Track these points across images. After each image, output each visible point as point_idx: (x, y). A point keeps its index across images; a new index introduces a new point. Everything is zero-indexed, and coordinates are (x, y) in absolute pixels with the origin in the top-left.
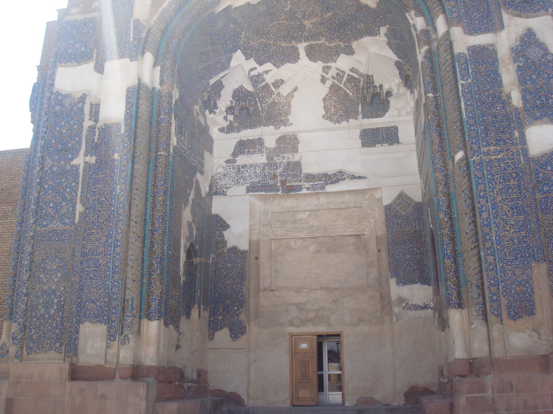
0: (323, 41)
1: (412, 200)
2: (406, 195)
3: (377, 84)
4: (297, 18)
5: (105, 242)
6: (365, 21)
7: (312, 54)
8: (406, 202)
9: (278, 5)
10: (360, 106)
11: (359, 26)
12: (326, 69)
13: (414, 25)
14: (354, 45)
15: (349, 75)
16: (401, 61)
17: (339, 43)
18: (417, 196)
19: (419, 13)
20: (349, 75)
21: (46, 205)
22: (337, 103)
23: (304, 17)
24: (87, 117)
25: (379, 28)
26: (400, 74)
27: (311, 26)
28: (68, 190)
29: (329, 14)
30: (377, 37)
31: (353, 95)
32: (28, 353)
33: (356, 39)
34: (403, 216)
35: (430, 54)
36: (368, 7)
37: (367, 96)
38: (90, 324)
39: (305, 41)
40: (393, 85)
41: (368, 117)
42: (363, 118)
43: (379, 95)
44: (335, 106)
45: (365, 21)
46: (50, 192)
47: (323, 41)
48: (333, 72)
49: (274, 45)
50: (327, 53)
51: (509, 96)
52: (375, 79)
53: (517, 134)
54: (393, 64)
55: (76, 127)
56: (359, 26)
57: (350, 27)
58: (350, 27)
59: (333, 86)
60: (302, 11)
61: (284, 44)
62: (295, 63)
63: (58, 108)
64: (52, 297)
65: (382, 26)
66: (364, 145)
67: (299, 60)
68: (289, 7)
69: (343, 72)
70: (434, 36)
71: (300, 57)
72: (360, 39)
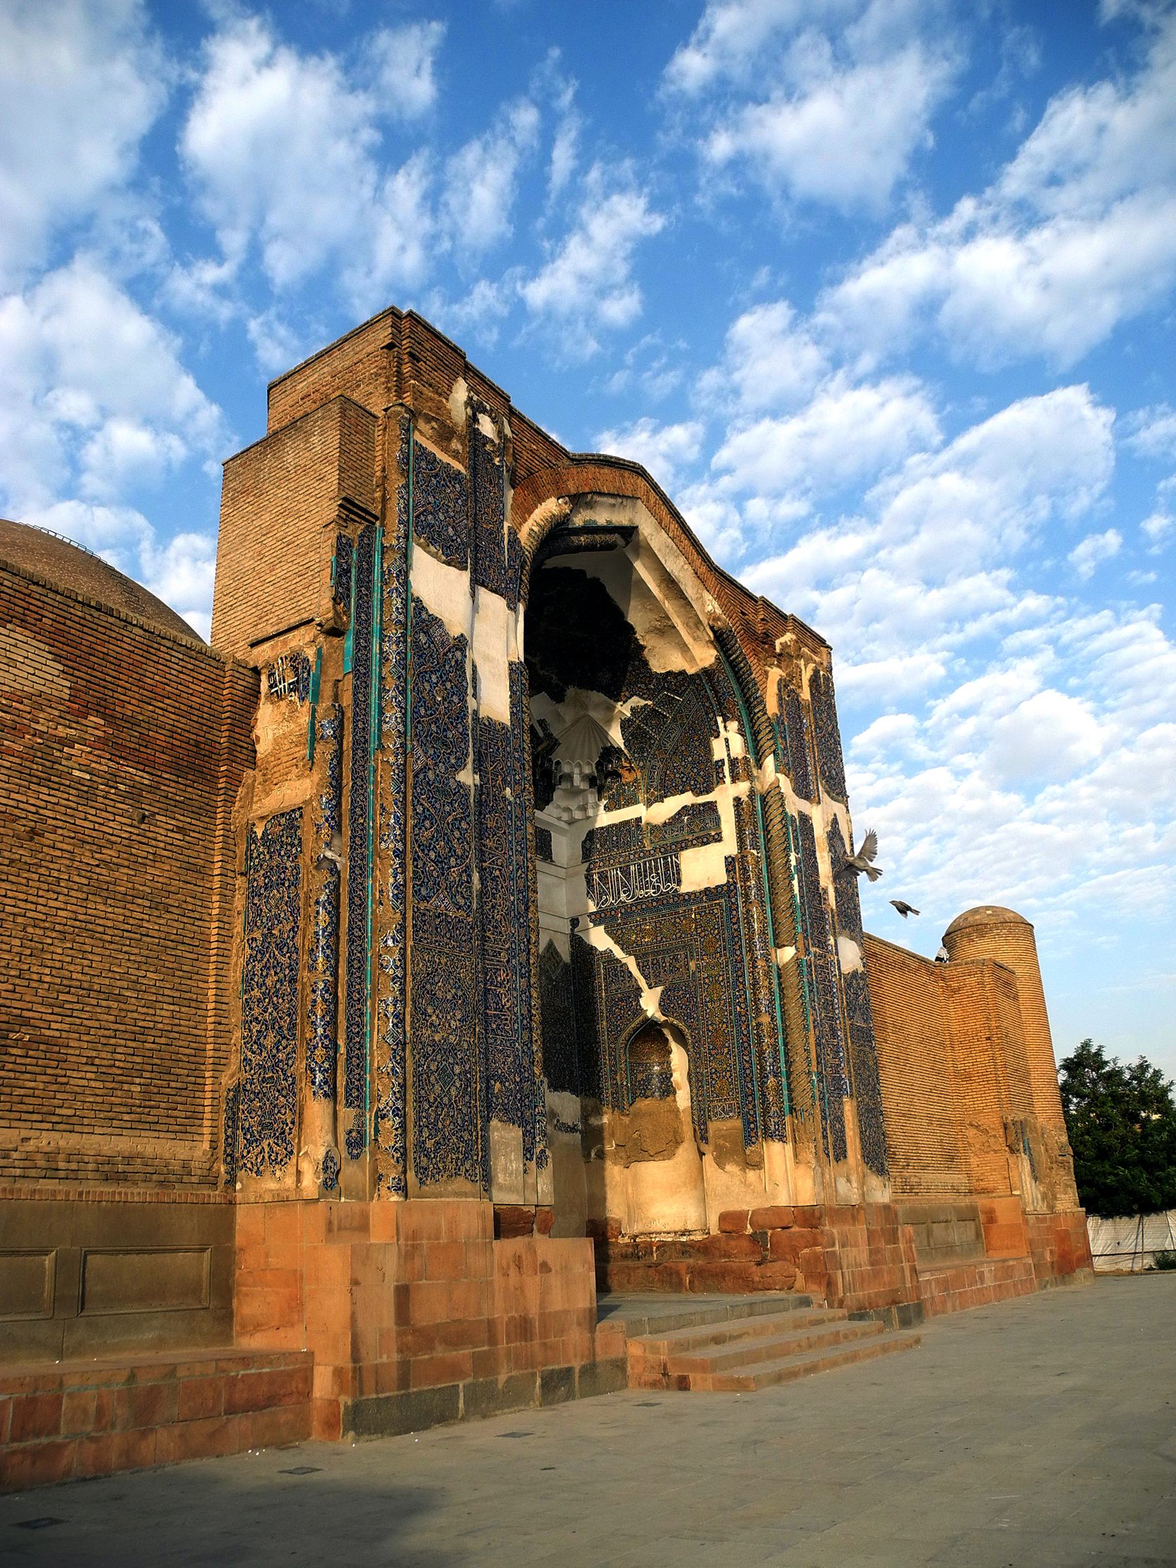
5: (508, 962)
13: (727, 740)
14: (571, 691)
16: (626, 751)
19: (741, 732)
21: (423, 851)
24: (470, 691)
28: (457, 834)
32: (422, 1182)
33: (580, 687)
35: (752, 794)
38: (499, 1124)
40: (576, 771)
46: (427, 824)
51: (825, 891)
53: (832, 941)
55: (455, 699)
63: (423, 638)
64: (451, 1060)
65: (641, 697)
70: (755, 772)
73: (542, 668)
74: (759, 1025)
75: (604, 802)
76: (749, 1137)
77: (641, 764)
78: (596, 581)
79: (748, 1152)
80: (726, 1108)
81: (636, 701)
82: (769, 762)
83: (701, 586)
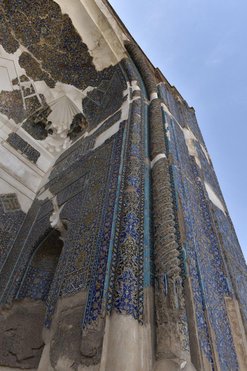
0: (40, 62)
1: (19, 207)
2: (16, 199)
3: (49, 118)
4: (40, 30)
6: (82, 75)
7: (24, 60)
8: (13, 204)
9: (40, 7)
10: (26, 120)
11: (73, 76)
12: (24, 79)
13: (131, 89)
14: (58, 84)
15: (36, 96)
17: (49, 74)
18: (25, 206)
20: (36, 96)
22: (10, 103)
23: (45, 35)
25: (88, 86)
26: (72, 125)
27: (42, 46)
29: (61, 52)
30: (81, 91)
31: (26, 110)
33: (63, 81)
34: (4, 213)
36: (95, 68)
37: (36, 119)
39: (29, 49)
40: (60, 128)
41: (26, 130)
42: (23, 127)
43: (44, 126)
44: (7, 103)
45: (82, 75)
47: (40, 62)
48: (26, 85)
49: (6, 24)
50: (35, 71)
52: (51, 114)
54: (73, 115)
56: (73, 76)
57: (66, 71)
58: (66, 71)
59: (16, 91)
60: (48, 30)
61: (13, 33)
62: (7, 52)
65: (91, 86)
66: (8, 141)
67: (11, 54)
68: (44, 18)
69: (34, 91)
71: (15, 53)
72: (66, 83)
73: (43, 68)
74: (124, 195)
75: (71, 141)
76: (91, 311)
77: (91, 120)
78: (66, 15)
79: (85, 333)
80: (79, 280)
81: (90, 89)
82: (155, 95)
83: (121, 30)
